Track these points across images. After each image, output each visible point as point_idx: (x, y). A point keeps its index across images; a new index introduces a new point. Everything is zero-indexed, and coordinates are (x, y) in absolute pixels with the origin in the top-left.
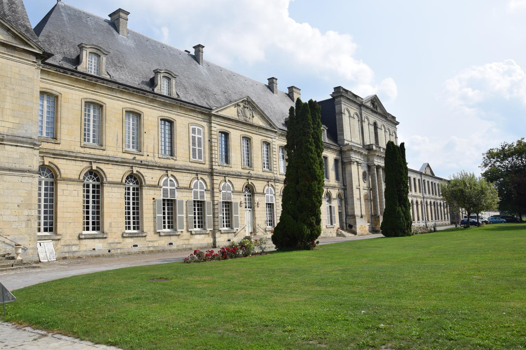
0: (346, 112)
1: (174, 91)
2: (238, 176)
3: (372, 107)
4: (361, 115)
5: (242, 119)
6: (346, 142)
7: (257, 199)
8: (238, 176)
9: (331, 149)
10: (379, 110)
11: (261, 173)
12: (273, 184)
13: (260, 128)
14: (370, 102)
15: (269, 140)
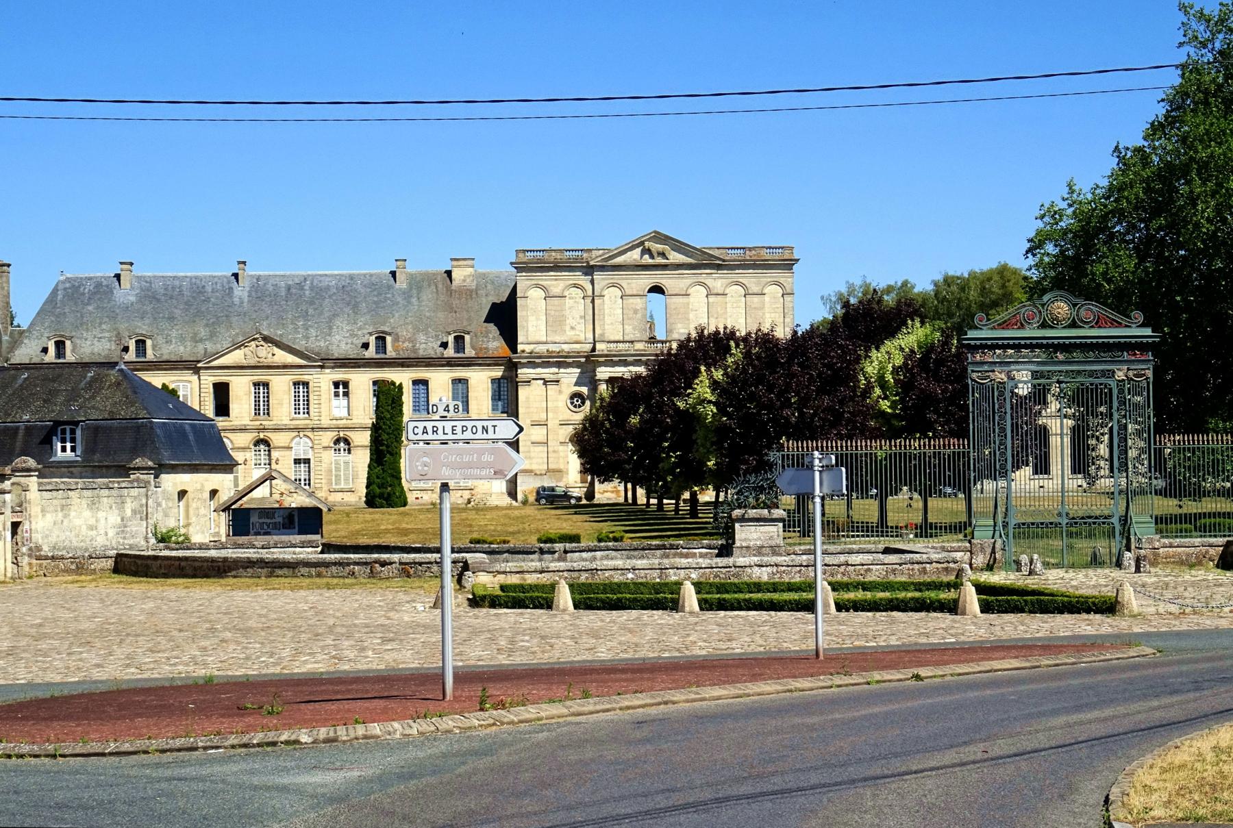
0: (536, 294)
1: (149, 352)
2: (243, 429)
3: (647, 256)
4: (592, 282)
5: (253, 362)
6: (520, 347)
7: (275, 454)
8: (243, 429)
9: (480, 365)
10: (675, 257)
11: (286, 421)
12: (309, 434)
13: (285, 367)
14: (639, 250)
15: (306, 378)
